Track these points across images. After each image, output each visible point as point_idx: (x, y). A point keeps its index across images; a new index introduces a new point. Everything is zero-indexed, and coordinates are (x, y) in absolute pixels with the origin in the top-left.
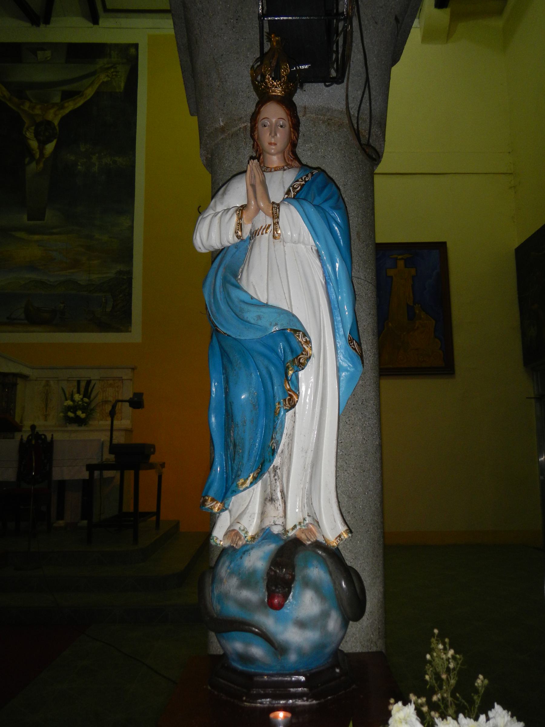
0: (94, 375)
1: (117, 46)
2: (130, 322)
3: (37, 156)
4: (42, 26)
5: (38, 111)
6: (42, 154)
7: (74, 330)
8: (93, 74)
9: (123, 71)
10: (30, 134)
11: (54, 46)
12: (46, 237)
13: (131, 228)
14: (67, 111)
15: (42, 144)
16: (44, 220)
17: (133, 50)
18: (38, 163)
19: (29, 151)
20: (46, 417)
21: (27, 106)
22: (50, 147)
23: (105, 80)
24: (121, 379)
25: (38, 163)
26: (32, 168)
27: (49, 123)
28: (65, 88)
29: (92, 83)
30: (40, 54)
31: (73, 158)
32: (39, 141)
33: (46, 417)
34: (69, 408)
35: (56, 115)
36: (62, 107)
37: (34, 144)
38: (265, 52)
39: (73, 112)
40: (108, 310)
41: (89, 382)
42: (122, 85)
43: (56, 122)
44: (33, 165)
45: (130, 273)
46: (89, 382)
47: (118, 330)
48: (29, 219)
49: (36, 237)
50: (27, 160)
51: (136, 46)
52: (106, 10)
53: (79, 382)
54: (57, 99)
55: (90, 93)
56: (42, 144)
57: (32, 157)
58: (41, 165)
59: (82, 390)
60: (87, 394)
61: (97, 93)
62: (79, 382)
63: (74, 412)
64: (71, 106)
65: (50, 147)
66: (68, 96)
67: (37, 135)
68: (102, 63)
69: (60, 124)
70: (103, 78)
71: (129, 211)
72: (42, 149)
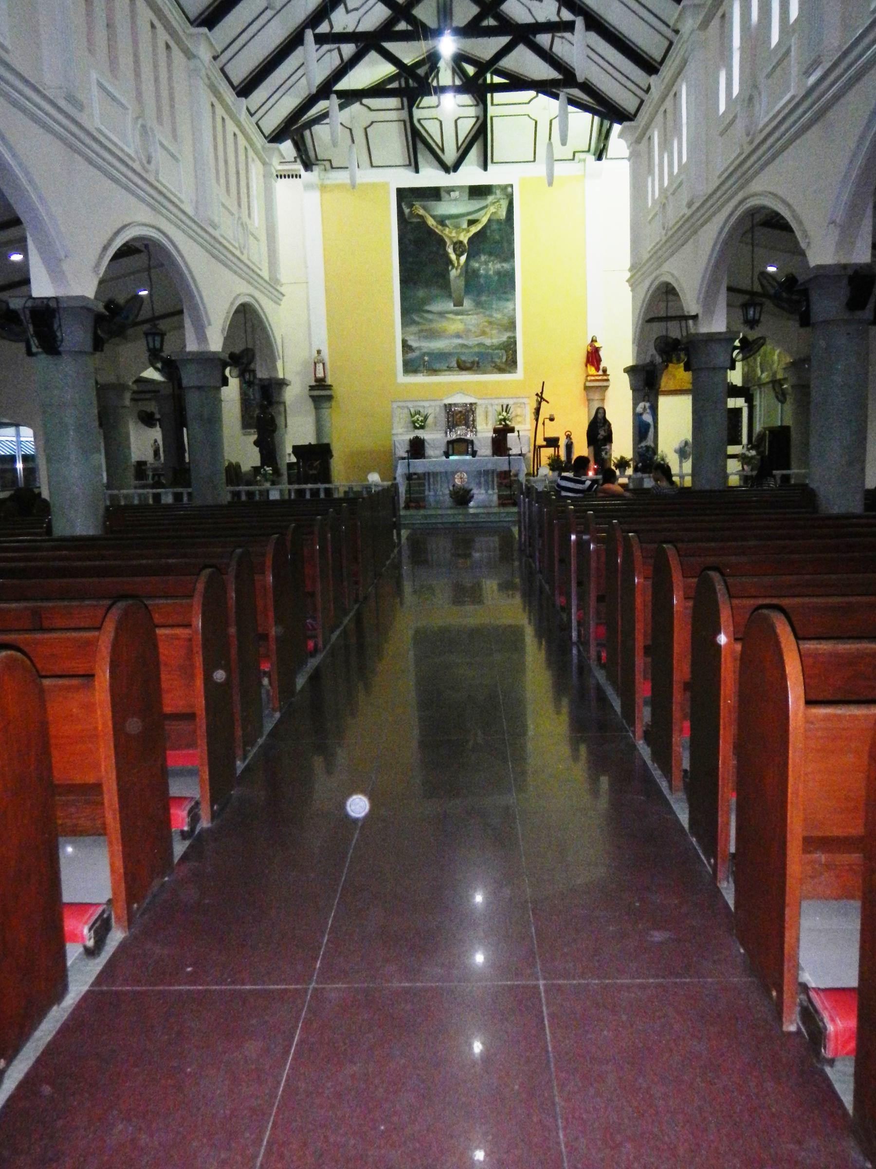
0: (510, 402)
1: (499, 186)
2: (516, 367)
3: (456, 265)
4: (452, 174)
5: (454, 234)
6: (458, 263)
7: (485, 373)
8: (486, 207)
9: (504, 204)
10: (450, 250)
11: (460, 188)
12: (465, 317)
13: (514, 309)
14: (471, 234)
15: (459, 256)
16: (462, 305)
17: (509, 189)
18: (457, 269)
19: (450, 262)
20: (487, 424)
21: (447, 231)
22: (463, 259)
23: (494, 210)
24: (524, 404)
25: (457, 269)
26: (454, 273)
27: (461, 242)
28: (470, 217)
29: (486, 213)
30: (452, 193)
31: (477, 265)
32: (456, 254)
33: (487, 424)
34: (501, 420)
35: (465, 237)
36: (468, 231)
37: (453, 256)
38: (560, 77)
39: (476, 234)
40: (504, 360)
41: (507, 406)
42: (504, 213)
43: (466, 241)
44: (454, 270)
45: (515, 337)
46: (507, 406)
47: (510, 372)
48: (455, 305)
49: (460, 317)
50: (450, 268)
51: (512, 186)
52: (492, 162)
53: (502, 406)
54: (465, 226)
55: (484, 220)
56: (459, 256)
57: (453, 266)
58: (459, 271)
59: (504, 410)
60: (507, 412)
61: (489, 220)
62: (502, 406)
63: (505, 421)
64: (475, 229)
65: (463, 259)
66: (471, 223)
67: (455, 250)
68: (491, 198)
69: (468, 243)
70: (492, 209)
71: (513, 299)
72: (458, 259)
